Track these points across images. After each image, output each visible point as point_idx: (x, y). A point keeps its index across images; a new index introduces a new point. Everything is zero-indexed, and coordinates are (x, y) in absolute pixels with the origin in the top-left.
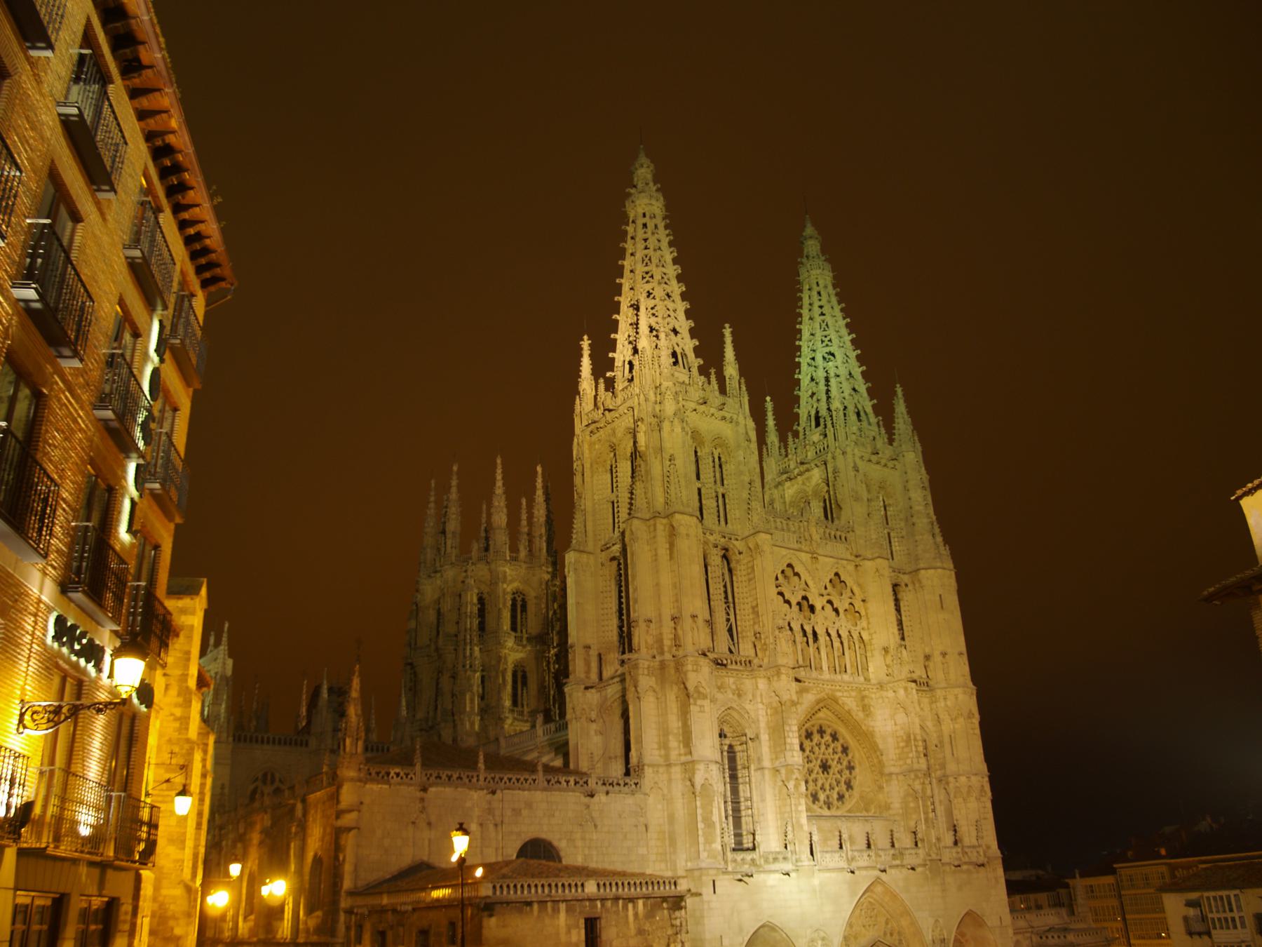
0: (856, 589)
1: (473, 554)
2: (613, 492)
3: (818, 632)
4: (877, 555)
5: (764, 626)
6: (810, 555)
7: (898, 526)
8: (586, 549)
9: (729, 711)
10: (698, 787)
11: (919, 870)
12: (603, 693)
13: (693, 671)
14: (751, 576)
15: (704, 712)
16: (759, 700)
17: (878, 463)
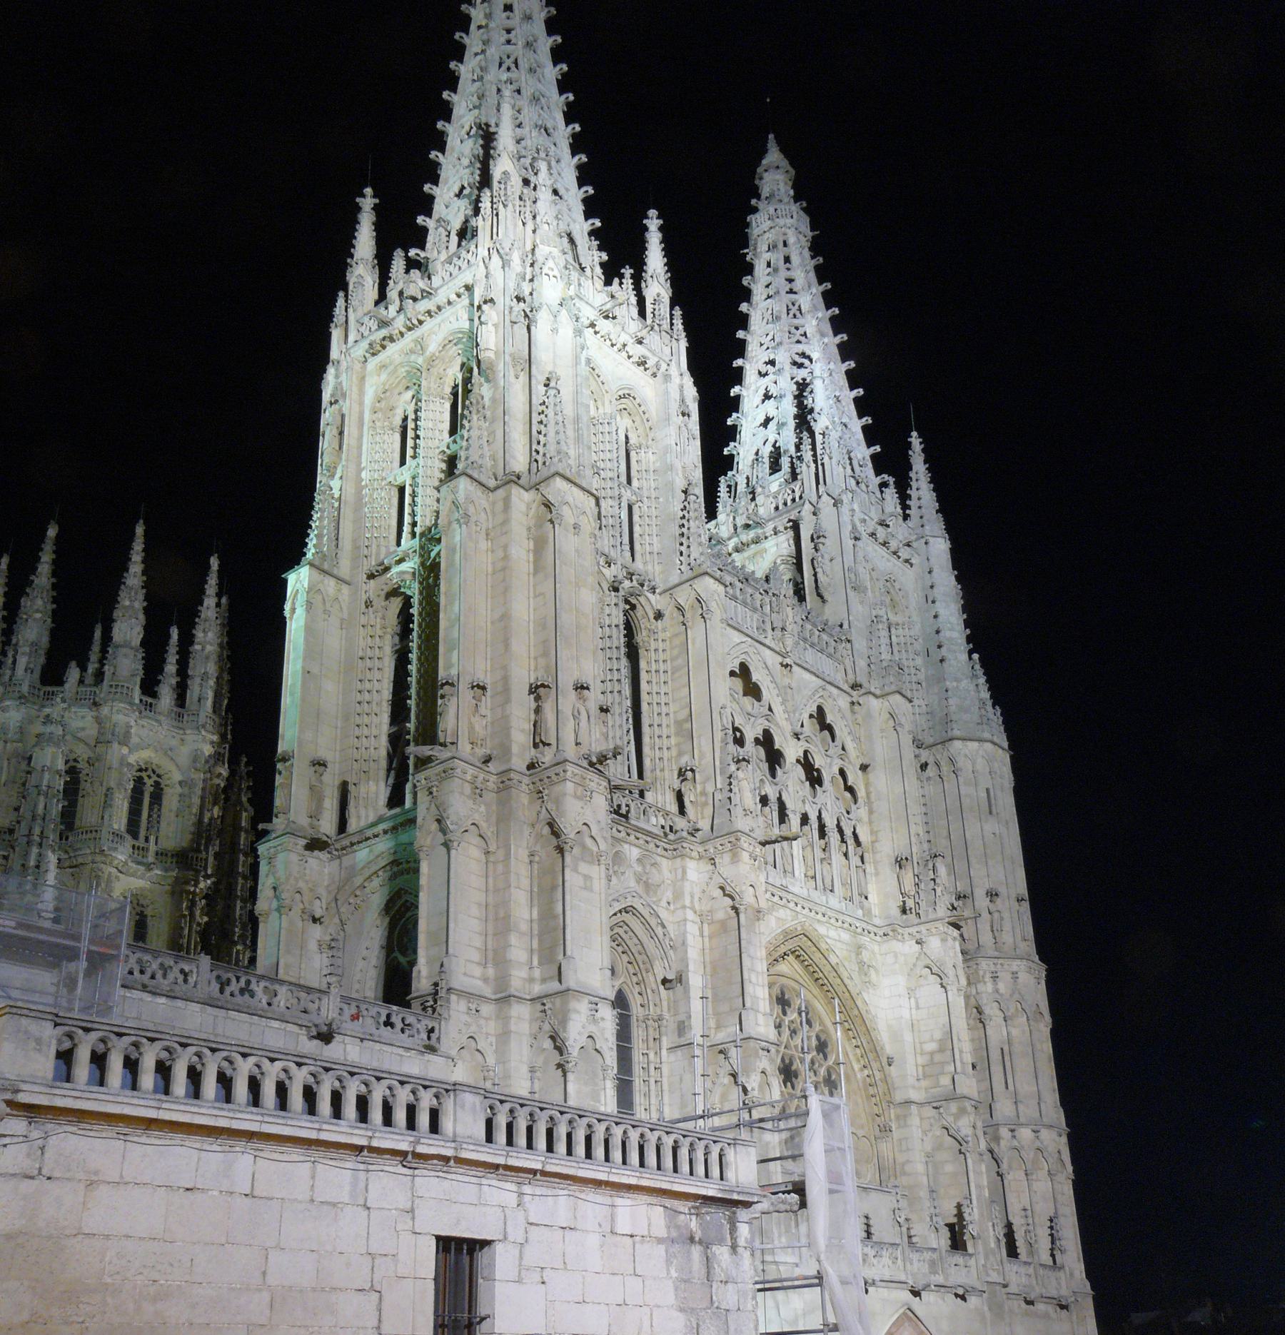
0: (850, 746)
1: (67, 686)
2: (403, 463)
3: (788, 805)
4: (893, 688)
5: (702, 756)
6: (780, 659)
7: (912, 664)
8: (335, 572)
9: (627, 917)
10: (574, 1051)
11: (973, 1300)
12: (347, 861)
13: (576, 797)
14: (680, 661)
15: (592, 891)
16: (687, 903)
17: (885, 544)
